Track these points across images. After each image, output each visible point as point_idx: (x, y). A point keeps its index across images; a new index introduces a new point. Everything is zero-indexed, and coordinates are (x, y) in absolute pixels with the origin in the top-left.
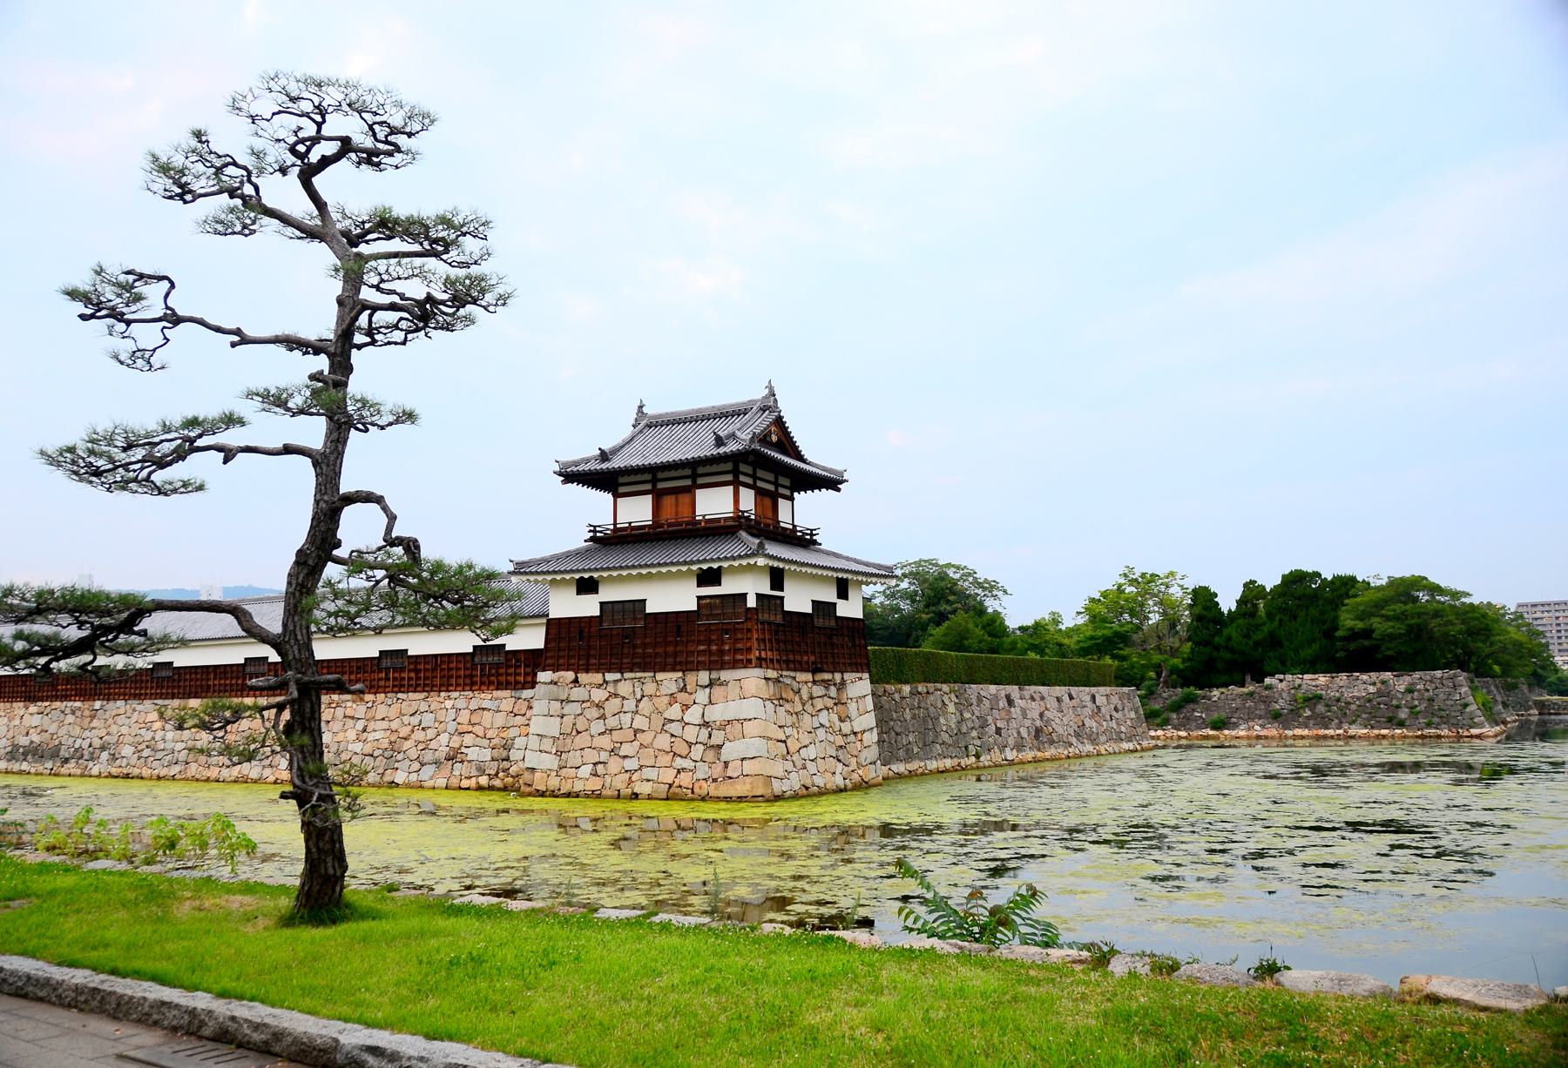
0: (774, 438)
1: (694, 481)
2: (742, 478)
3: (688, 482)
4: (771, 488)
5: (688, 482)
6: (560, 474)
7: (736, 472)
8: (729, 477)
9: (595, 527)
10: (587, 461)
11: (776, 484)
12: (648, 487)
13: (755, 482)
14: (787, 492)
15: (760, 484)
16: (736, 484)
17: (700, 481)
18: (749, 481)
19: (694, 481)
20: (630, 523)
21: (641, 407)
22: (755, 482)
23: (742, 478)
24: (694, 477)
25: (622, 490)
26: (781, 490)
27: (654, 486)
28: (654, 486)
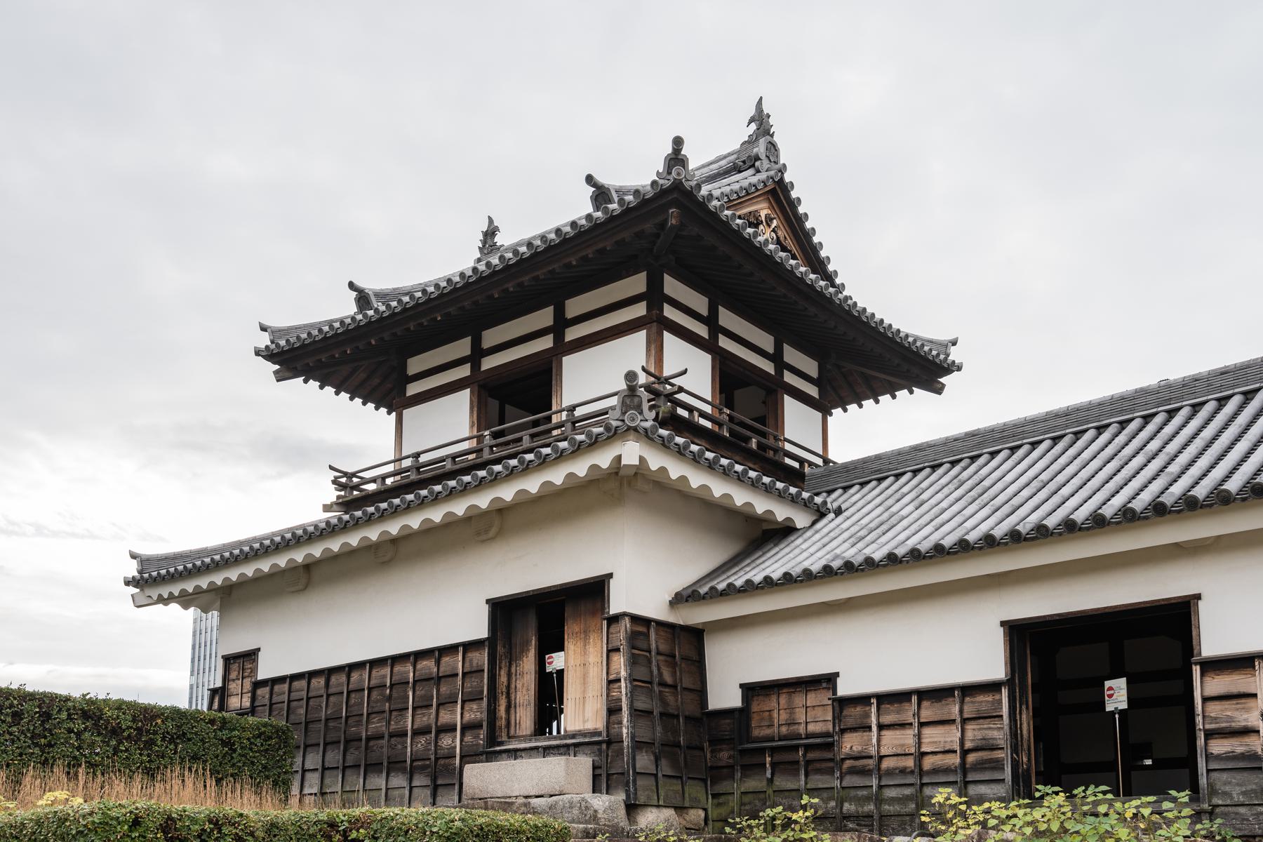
1: (559, 337)
2: (669, 312)
3: (546, 343)
9: (350, 476)
12: (464, 371)
16: (656, 325)
18: (702, 331)
19: (559, 337)
20: (417, 455)
21: (490, 233)
24: (561, 323)
27: (476, 366)
28: (476, 366)
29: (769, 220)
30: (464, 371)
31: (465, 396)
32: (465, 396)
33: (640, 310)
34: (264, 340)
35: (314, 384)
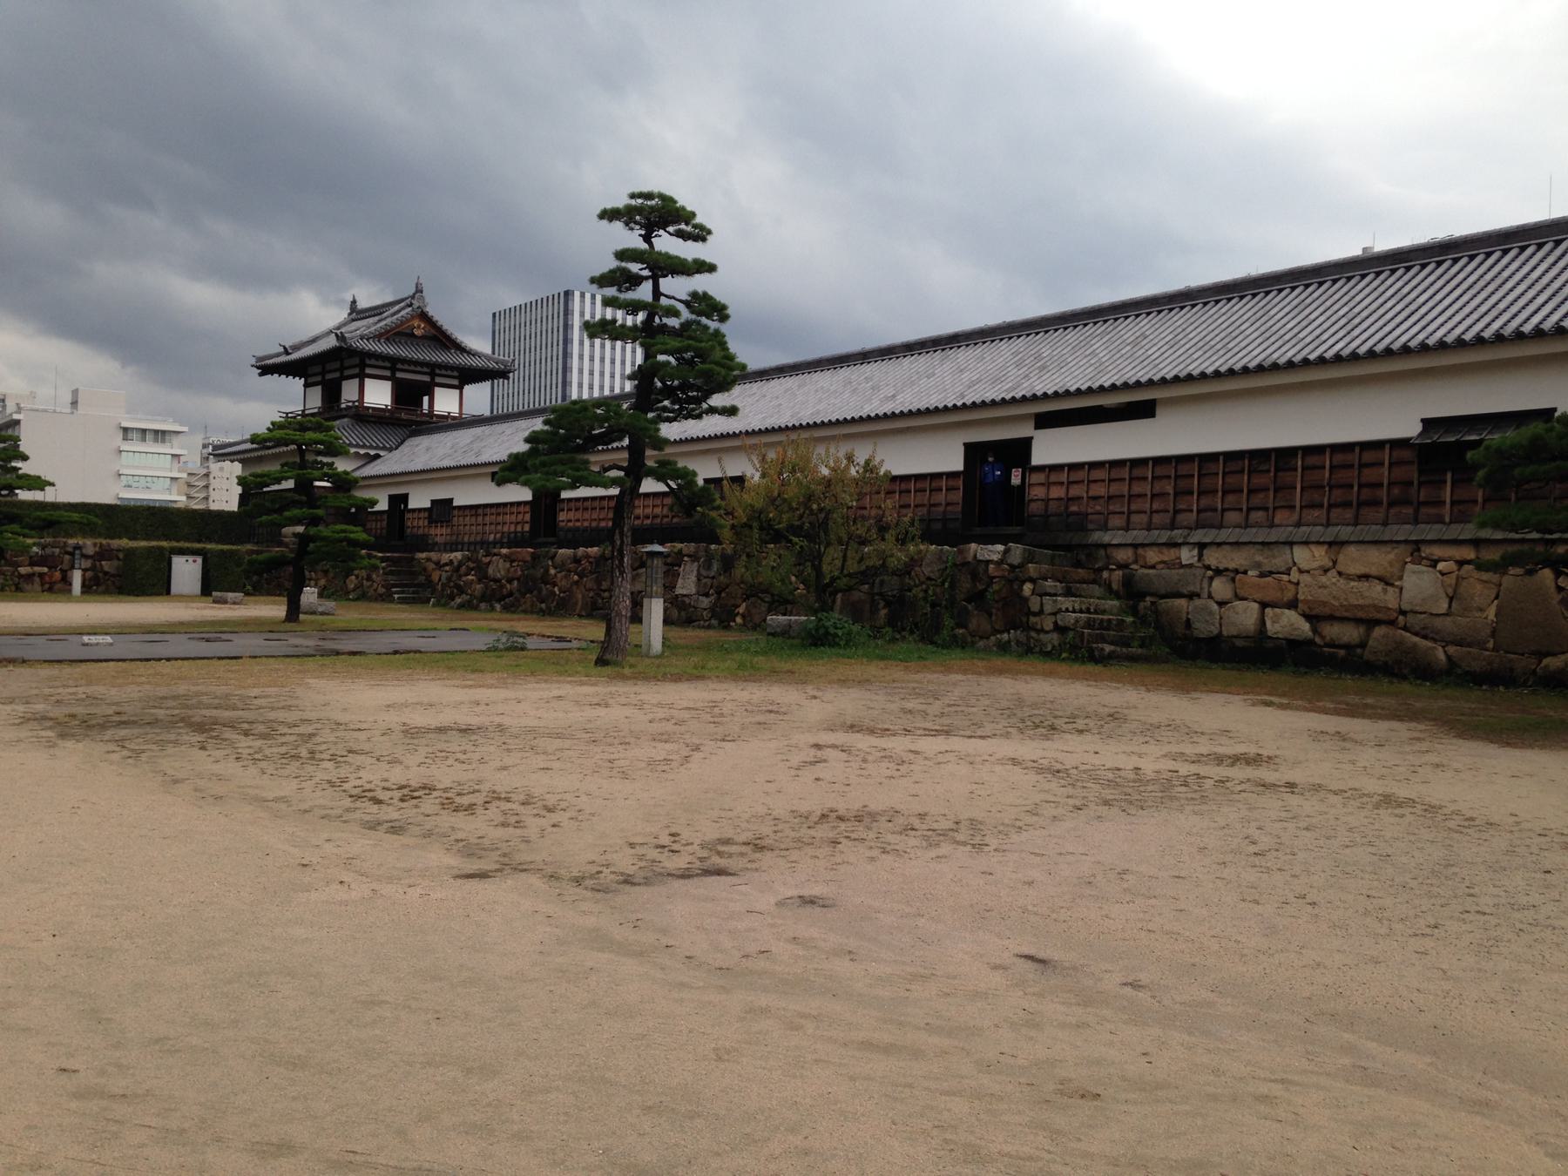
0: (417, 332)
1: (342, 373)
3: (337, 375)
4: (426, 378)
5: (337, 375)
6: (258, 368)
7: (363, 366)
8: (357, 371)
9: (287, 414)
10: (278, 355)
11: (433, 375)
12: (319, 378)
13: (393, 374)
14: (456, 382)
15: (399, 375)
17: (347, 373)
18: (388, 373)
19: (342, 373)
22: (393, 374)
23: (368, 371)
24: (342, 369)
25: (311, 380)
26: (438, 380)
27: (323, 377)
28: (323, 377)
29: (419, 327)
30: (319, 378)
31: (319, 388)
32: (319, 388)
33: (357, 371)
34: (253, 361)
35: (276, 375)
